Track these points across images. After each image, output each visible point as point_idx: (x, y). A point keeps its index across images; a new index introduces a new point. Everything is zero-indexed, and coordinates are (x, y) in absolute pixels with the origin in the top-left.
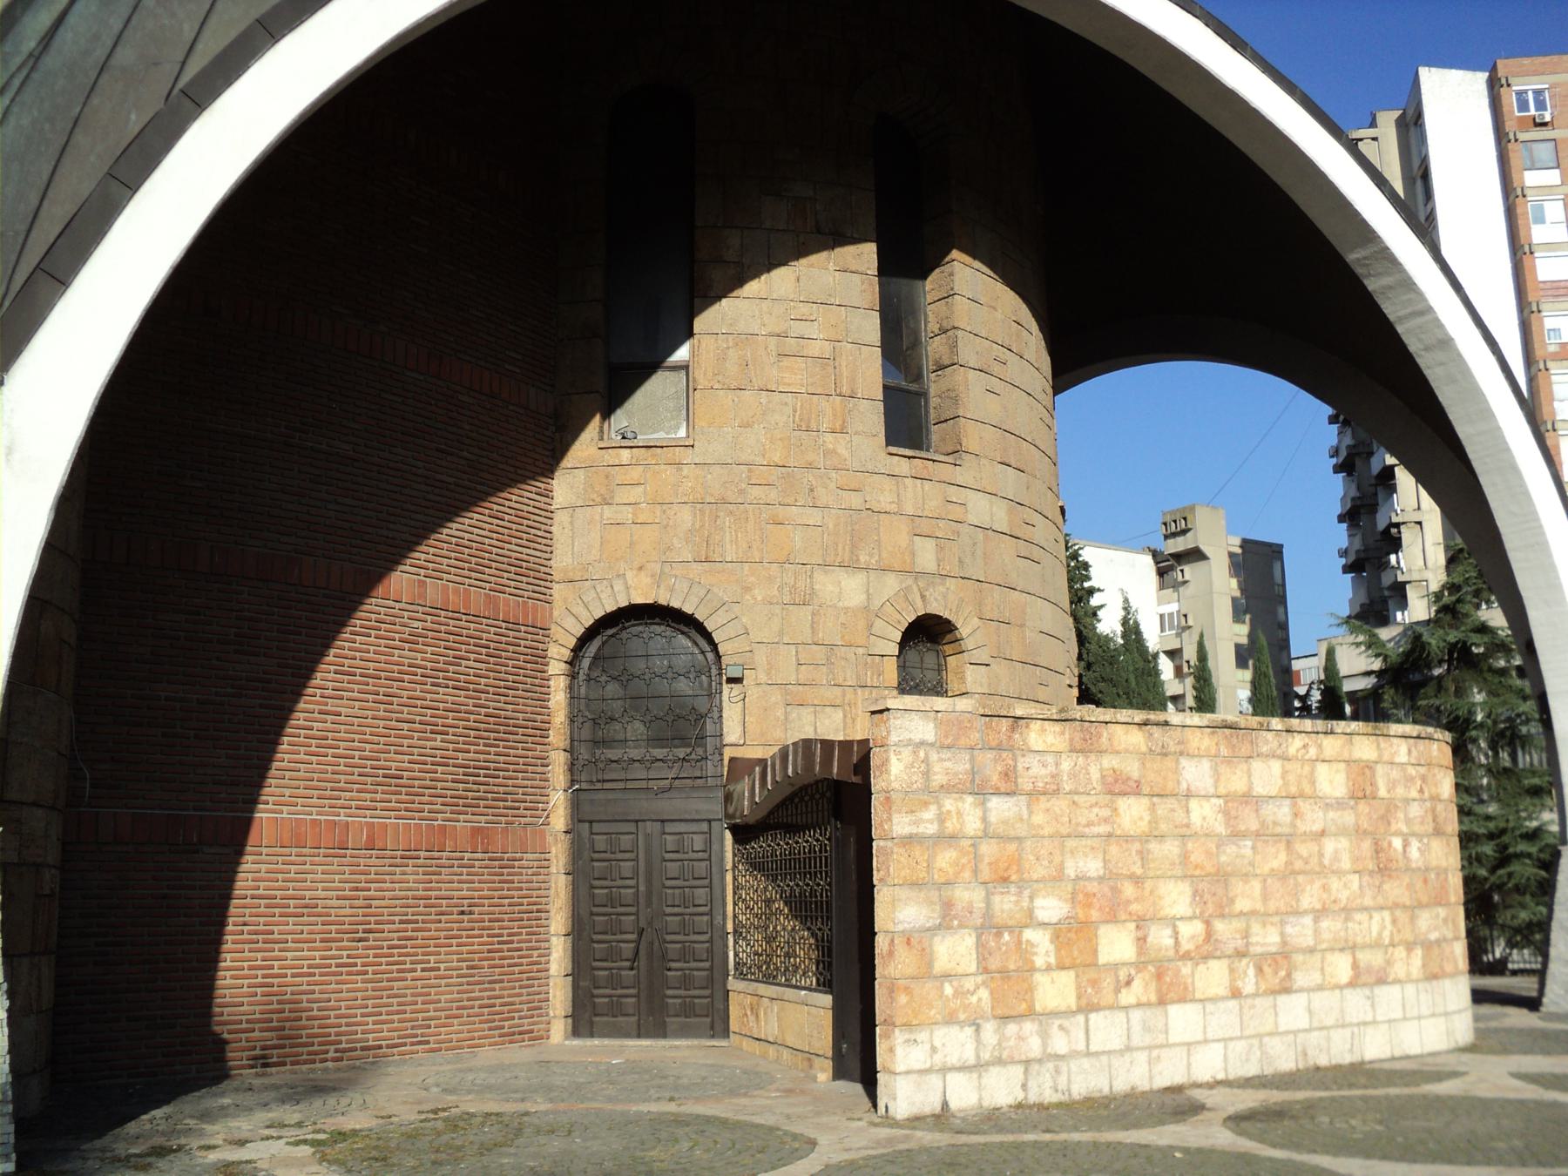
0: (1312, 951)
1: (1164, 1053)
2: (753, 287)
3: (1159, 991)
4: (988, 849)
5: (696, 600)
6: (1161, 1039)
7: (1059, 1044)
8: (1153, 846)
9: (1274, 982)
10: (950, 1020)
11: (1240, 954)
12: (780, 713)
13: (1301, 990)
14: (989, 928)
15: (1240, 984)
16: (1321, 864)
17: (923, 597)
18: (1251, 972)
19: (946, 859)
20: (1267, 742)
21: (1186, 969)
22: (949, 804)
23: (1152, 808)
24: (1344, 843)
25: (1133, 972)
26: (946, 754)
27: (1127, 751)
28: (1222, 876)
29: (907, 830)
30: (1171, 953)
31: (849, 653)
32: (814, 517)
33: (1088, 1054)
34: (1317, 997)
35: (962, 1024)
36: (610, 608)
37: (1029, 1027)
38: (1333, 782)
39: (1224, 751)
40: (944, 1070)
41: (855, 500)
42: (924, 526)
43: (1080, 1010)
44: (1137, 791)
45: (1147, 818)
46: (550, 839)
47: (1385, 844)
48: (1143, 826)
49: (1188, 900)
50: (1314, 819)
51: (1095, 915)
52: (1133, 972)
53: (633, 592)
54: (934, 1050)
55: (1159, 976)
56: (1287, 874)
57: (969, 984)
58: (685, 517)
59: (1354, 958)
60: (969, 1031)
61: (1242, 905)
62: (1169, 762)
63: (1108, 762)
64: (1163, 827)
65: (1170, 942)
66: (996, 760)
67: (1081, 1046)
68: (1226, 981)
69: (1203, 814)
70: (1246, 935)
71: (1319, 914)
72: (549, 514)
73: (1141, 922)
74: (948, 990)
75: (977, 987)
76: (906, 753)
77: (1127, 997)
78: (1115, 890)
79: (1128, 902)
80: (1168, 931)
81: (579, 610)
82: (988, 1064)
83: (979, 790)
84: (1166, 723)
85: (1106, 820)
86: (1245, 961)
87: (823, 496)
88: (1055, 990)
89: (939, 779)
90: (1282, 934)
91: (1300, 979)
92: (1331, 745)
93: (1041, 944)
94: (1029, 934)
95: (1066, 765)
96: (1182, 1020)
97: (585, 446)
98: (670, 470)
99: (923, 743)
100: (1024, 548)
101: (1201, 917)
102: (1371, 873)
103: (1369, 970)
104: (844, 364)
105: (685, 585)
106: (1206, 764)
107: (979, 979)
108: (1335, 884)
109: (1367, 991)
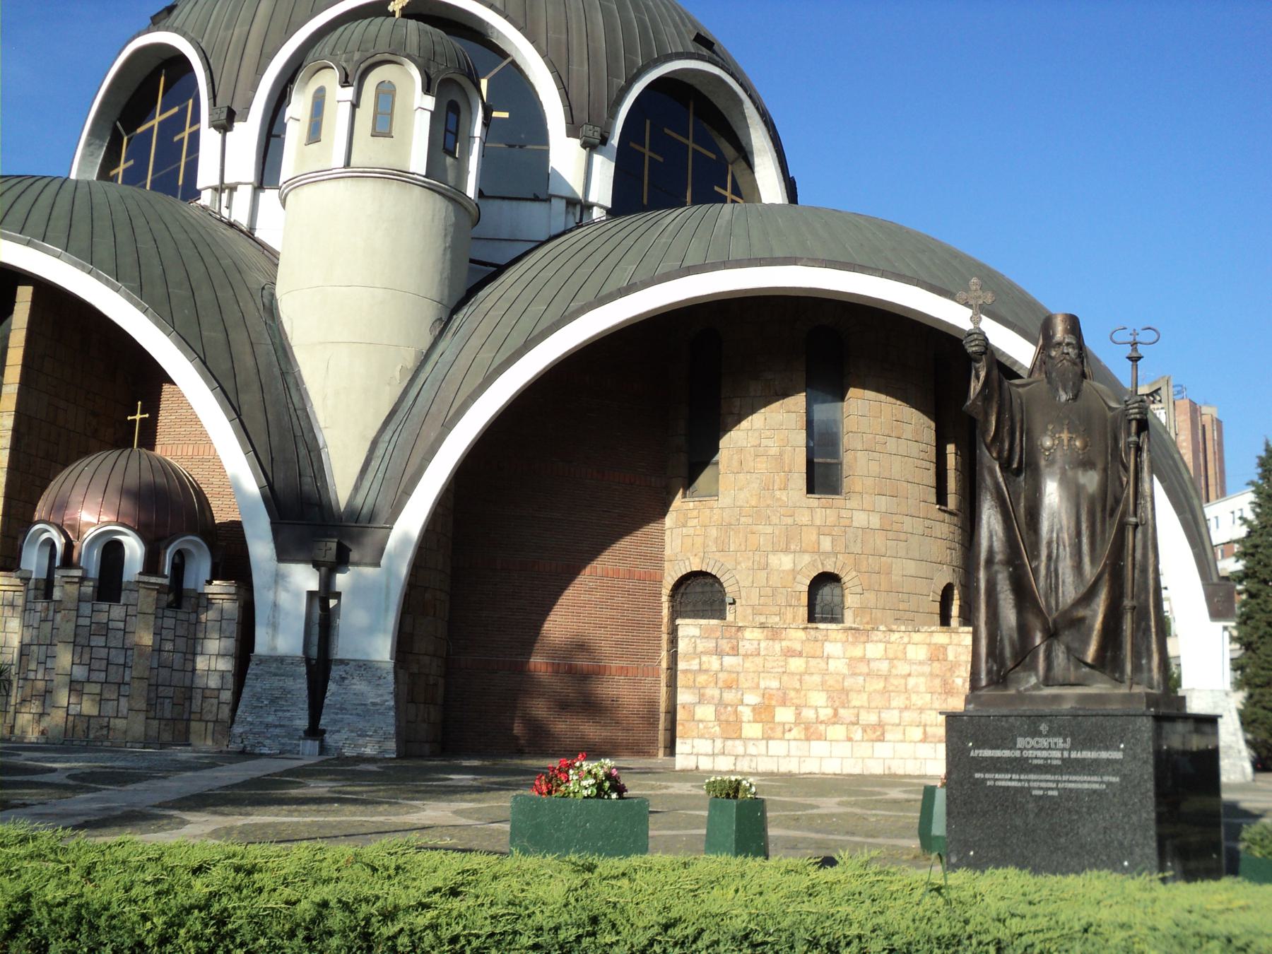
0: (899, 725)
1: (807, 759)
2: (745, 424)
3: (806, 735)
4: (722, 676)
5: (716, 569)
6: (807, 754)
7: (752, 749)
8: (806, 677)
9: (874, 736)
10: (701, 737)
11: (853, 724)
12: (751, 618)
13: (890, 741)
14: (721, 704)
15: (852, 736)
16: (906, 688)
17: (822, 564)
18: (860, 731)
19: (702, 679)
20: (877, 636)
21: (822, 727)
22: (704, 658)
23: (807, 663)
24: (922, 680)
25: (793, 726)
26: (703, 640)
27: (795, 639)
28: (845, 692)
29: (685, 668)
30: (815, 721)
31: (784, 591)
32: (769, 530)
33: (767, 756)
34: (899, 745)
35: (706, 739)
36: (684, 573)
37: (738, 742)
38: (918, 652)
39: (850, 639)
40: (697, 755)
41: (790, 521)
42: (826, 530)
43: (763, 739)
44: (800, 654)
45: (804, 666)
46: (661, 672)
47: (950, 681)
48: (802, 669)
49: (825, 700)
50: (903, 668)
51: (773, 703)
52: (793, 726)
53: (693, 565)
54: (693, 747)
55: (807, 729)
56: (885, 691)
57: (711, 725)
58: (714, 532)
59: (925, 730)
60: (710, 742)
61: (857, 703)
62: (819, 644)
63: (784, 644)
64: (812, 670)
65: (815, 716)
66: (728, 643)
67: (764, 752)
68: (845, 734)
69: (838, 666)
70: (858, 716)
71: (902, 710)
72: (663, 531)
73: (797, 707)
74: (701, 726)
75: (714, 726)
76: (686, 640)
77: (787, 736)
78: (785, 693)
79: (792, 699)
80: (814, 711)
81: (673, 573)
82: (717, 755)
83: (719, 653)
84: (817, 628)
85: (782, 667)
86: (856, 727)
87: (775, 520)
88: (752, 730)
89: (700, 648)
90: (879, 717)
91: (888, 736)
92: (917, 637)
93: (746, 713)
94: (740, 708)
95: (763, 644)
96: (816, 746)
97: (678, 502)
98: (708, 511)
99: (693, 636)
100: (890, 534)
101: (832, 706)
102: (940, 694)
103: (934, 736)
104: (786, 457)
105: (714, 562)
106: (839, 645)
107: (716, 723)
108: (914, 698)
109: (932, 745)
